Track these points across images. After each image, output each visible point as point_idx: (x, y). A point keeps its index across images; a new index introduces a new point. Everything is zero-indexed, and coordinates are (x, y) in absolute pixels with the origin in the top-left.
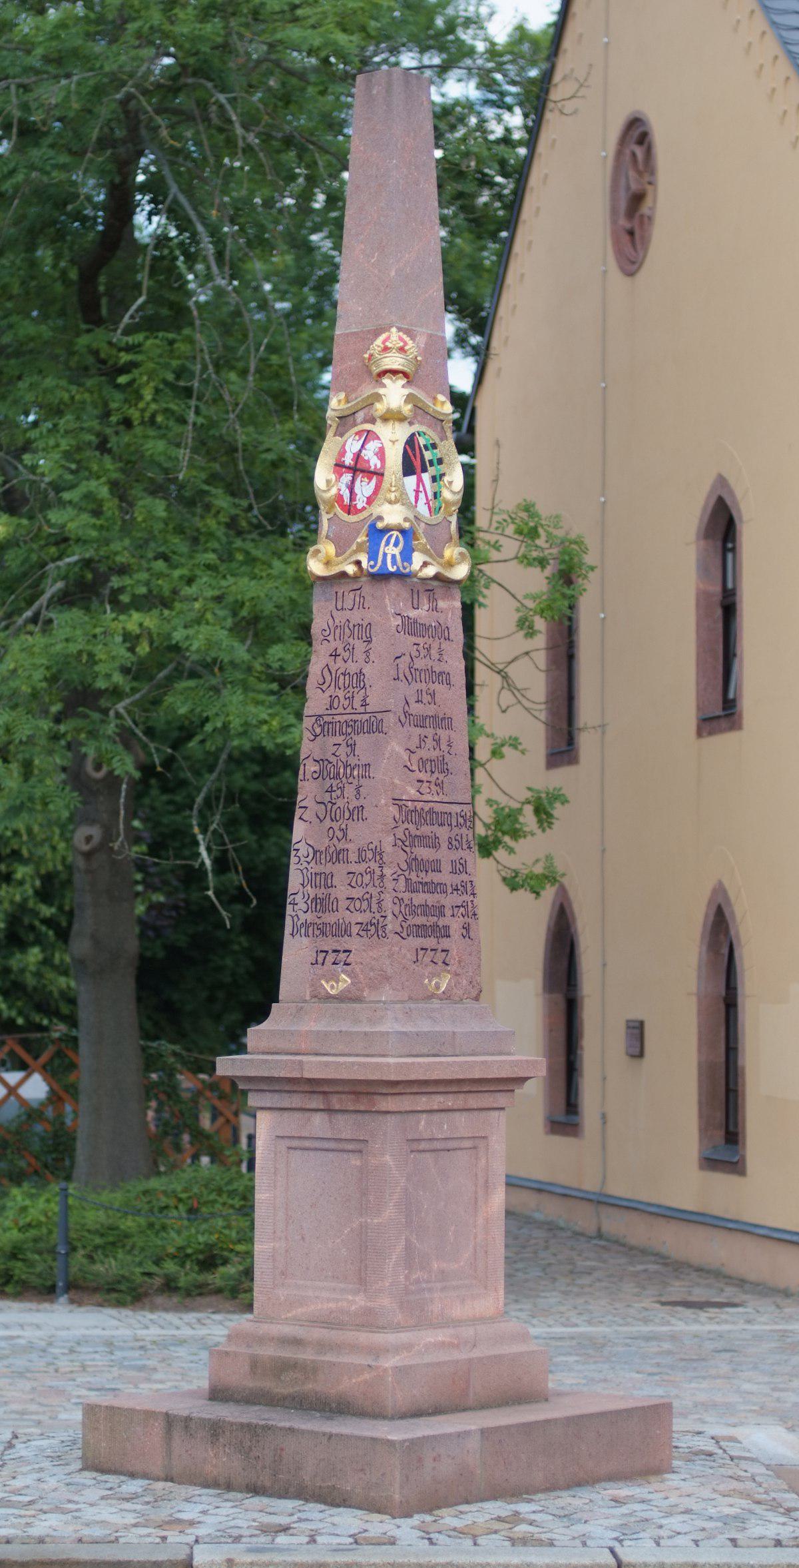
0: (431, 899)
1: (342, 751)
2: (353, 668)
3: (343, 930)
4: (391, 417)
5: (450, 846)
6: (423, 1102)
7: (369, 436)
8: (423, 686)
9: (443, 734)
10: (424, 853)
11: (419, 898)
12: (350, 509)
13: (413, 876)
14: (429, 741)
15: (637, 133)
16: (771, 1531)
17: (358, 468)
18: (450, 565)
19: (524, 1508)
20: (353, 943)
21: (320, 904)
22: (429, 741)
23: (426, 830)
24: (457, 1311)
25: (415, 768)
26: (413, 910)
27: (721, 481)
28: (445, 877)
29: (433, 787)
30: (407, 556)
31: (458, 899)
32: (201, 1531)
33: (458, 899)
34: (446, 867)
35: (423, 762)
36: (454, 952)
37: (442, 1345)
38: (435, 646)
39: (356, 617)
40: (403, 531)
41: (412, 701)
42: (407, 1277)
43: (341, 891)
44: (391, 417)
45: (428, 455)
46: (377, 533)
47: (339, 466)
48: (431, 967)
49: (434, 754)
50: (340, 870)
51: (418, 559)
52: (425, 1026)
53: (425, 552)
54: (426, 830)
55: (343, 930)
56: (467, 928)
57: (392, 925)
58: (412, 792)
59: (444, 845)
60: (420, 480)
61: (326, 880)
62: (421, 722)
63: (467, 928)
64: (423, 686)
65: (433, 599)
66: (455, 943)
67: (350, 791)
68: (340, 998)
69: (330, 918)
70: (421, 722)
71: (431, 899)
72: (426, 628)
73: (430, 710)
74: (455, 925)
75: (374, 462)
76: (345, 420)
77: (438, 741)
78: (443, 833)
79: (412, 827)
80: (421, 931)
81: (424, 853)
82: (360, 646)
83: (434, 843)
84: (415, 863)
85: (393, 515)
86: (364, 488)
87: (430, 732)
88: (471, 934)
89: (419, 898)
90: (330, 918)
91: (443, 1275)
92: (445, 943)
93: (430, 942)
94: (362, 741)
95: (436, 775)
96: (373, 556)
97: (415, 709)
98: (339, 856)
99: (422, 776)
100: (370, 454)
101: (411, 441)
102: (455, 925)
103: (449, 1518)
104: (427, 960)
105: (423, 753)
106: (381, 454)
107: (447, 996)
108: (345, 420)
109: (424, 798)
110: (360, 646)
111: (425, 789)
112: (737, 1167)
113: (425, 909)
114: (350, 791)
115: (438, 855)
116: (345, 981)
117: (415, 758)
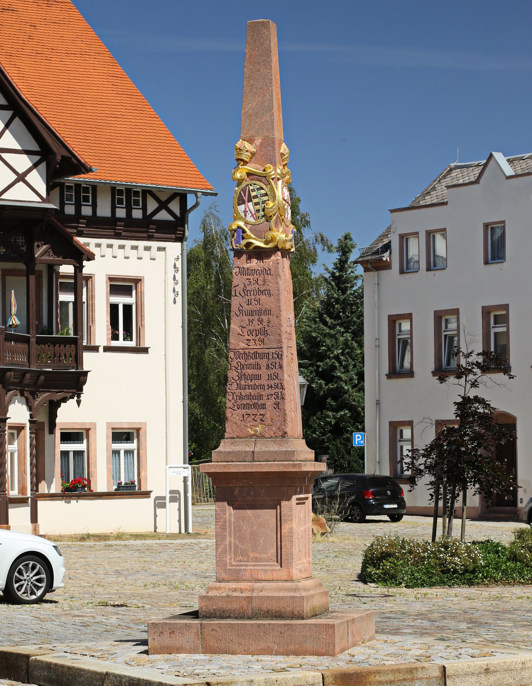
0: (253, 392)
5: (268, 367)
9: (265, 318)
10: (250, 372)
13: (243, 382)
14: (256, 322)
23: (252, 361)
24: (262, 576)
25: (246, 334)
26: (241, 397)
28: (264, 381)
29: (257, 342)
34: (265, 377)
35: (250, 332)
38: (261, 278)
41: (244, 305)
48: (254, 423)
56: (277, 404)
58: (243, 345)
66: (269, 412)
70: (251, 313)
71: (253, 392)
74: (270, 403)
77: (261, 321)
78: (263, 362)
79: (242, 361)
80: (245, 406)
83: (258, 367)
92: (262, 412)
93: (255, 411)
95: (259, 336)
97: (246, 307)
99: (249, 338)
105: (251, 328)
109: (250, 347)
111: (252, 343)
113: (249, 397)
115: (260, 372)
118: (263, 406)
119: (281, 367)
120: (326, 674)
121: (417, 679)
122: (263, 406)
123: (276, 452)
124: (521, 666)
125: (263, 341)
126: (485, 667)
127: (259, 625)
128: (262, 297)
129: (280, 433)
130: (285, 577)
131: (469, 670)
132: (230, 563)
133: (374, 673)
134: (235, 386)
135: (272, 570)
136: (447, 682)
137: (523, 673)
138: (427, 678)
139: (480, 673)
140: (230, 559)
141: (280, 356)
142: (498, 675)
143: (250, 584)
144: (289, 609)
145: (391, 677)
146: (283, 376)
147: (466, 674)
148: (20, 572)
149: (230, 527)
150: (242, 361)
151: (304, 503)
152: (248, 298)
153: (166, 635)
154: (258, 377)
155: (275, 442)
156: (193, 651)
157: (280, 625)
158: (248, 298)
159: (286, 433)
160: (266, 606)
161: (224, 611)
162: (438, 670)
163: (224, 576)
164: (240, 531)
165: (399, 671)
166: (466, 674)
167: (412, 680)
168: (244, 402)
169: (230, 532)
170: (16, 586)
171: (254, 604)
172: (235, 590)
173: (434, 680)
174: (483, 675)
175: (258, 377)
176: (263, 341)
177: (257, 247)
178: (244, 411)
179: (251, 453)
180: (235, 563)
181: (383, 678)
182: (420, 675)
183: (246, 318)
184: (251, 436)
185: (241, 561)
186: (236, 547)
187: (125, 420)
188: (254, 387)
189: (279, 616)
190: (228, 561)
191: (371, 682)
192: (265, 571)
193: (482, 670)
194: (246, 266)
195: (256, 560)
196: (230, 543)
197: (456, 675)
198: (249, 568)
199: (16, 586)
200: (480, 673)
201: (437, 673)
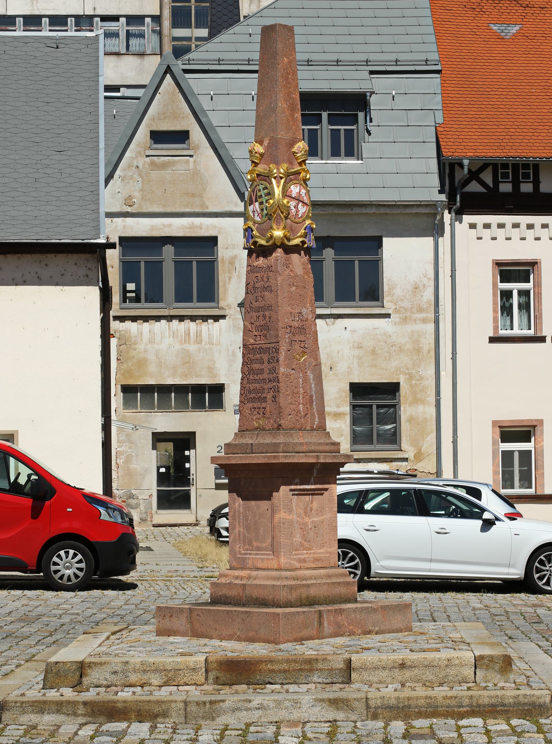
5: (269, 362)
9: (267, 313)
10: (256, 366)
13: (251, 377)
14: (261, 318)
22: (261, 318)
24: (260, 565)
25: (254, 330)
26: (250, 392)
29: (262, 337)
31: (270, 385)
33: (270, 385)
36: (268, 409)
41: (253, 302)
49: (262, 323)
58: (252, 341)
59: (266, 362)
63: (274, 397)
66: (269, 406)
70: (258, 309)
74: (269, 396)
77: (264, 316)
78: (265, 357)
81: (256, 366)
87: (261, 313)
88: (277, 400)
92: (264, 405)
95: (263, 332)
97: (256, 304)
102: (269, 396)
104: (255, 413)
105: (258, 324)
109: (257, 343)
113: (255, 390)
117: (253, 326)
118: (264, 399)
119: (278, 361)
120: (211, 659)
121: (317, 670)
122: (264, 399)
123: (268, 444)
124: (446, 662)
125: (265, 336)
126: (401, 662)
127: (228, 612)
128: (266, 293)
129: (276, 426)
130: (276, 567)
131: (379, 663)
132: (240, 551)
133: (266, 661)
135: (268, 559)
136: (352, 675)
137: (448, 670)
138: (328, 669)
139: (394, 667)
140: (240, 548)
141: (277, 351)
142: (416, 671)
143: (248, 572)
144: (271, 597)
145: (285, 666)
146: (279, 369)
147: (376, 668)
148: (542, 562)
149: (239, 517)
150: (251, 356)
151: (322, 494)
152: (256, 295)
153: (167, 618)
154: (261, 371)
155: (271, 434)
156: (183, 635)
157: (242, 612)
158: (256, 295)
159: (280, 425)
160: (256, 593)
161: (227, 598)
162: (342, 662)
163: (234, 564)
164: (247, 520)
165: (295, 661)
166: (376, 668)
167: (311, 670)
168: (252, 396)
169: (239, 522)
170: (536, 576)
171: (248, 592)
172: (237, 578)
173: (337, 672)
174: (398, 670)
175: (261, 371)
176: (265, 336)
177: (261, 246)
179: (250, 446)
180: (243, 552)
181: (276, 667)
182: (320, 666)
183: (254, 314)
184: (256, 429)
185: (247, 550)
186: (244, 536)
187: (517, 413)
189: (263, 603)
190: (238, 549)
191: (261, 670)
192: (263, 560)
193: (396, 665)
194: (256, 264)
196: (239, 531)
197: (364, 668)
198: (254, 558)
199: (536, 576)
200: (394, 667)
201: (342, 666)
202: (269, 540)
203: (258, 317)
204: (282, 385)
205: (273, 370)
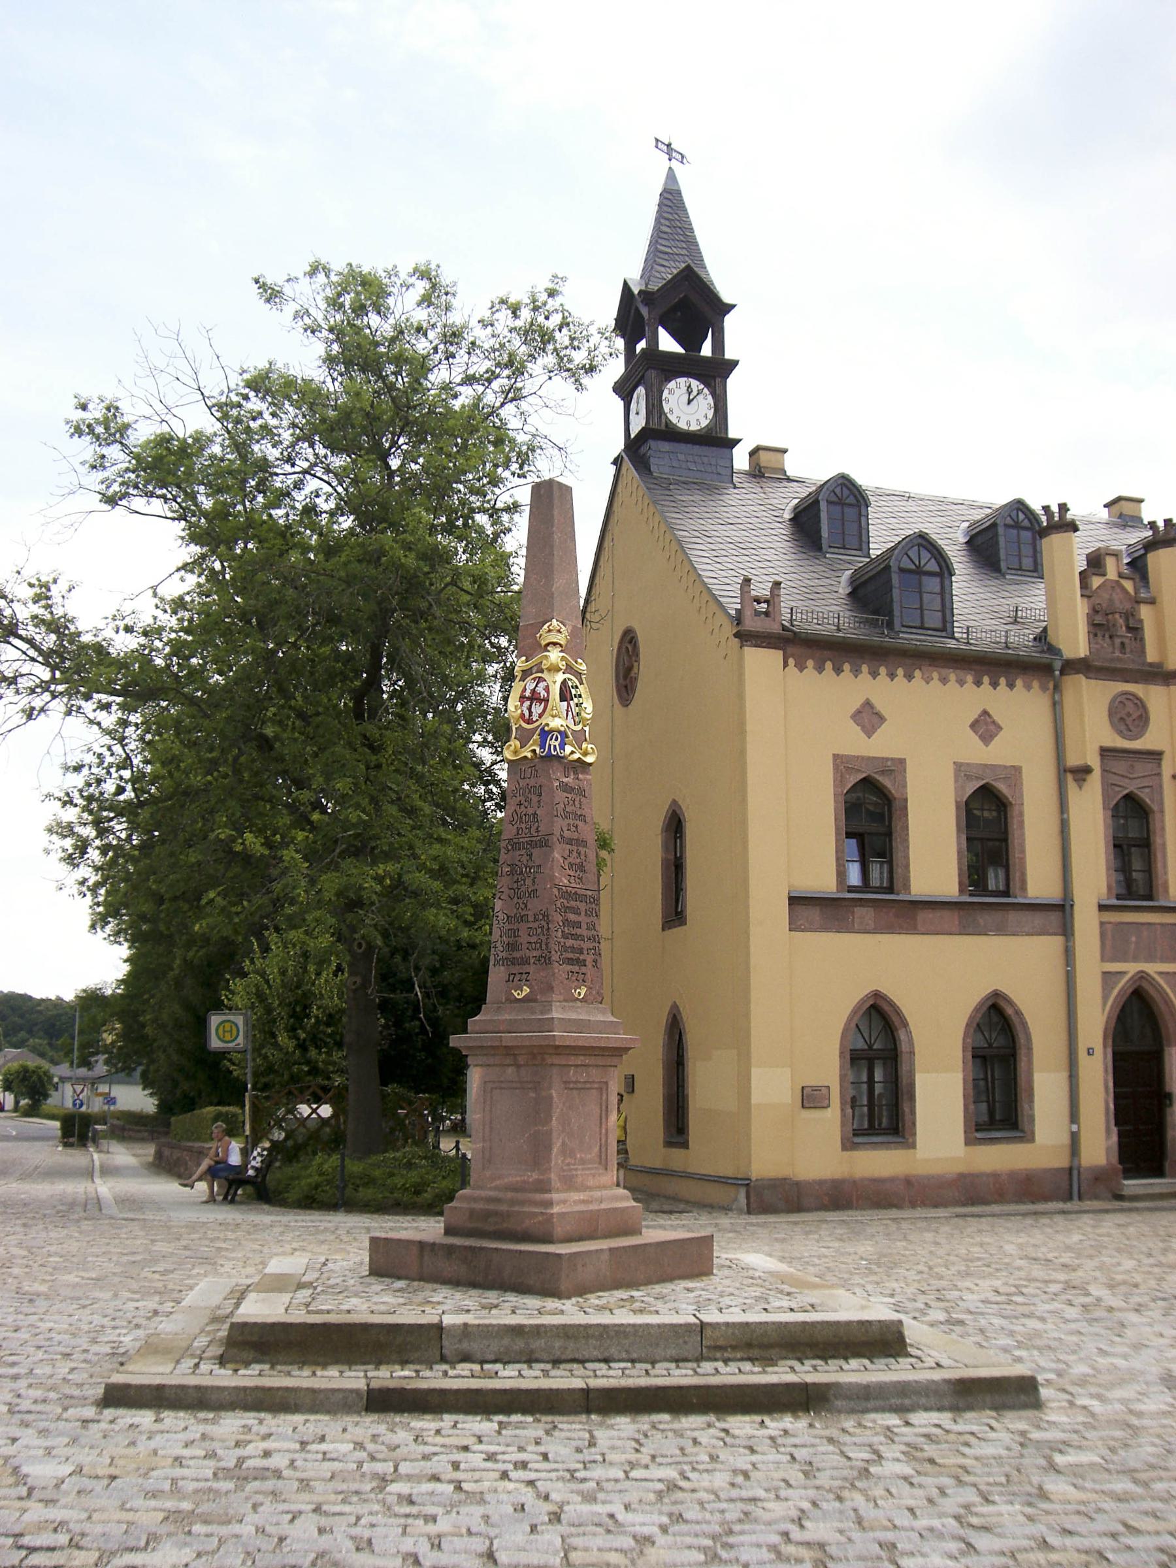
0: (576, 943)
1: (524, 859)
2: (530, 811)
3: (525, 961)
4: (555, 669)
6: (573, 1060)
7: (541, 679)
8: (571, 822)
10: (572, 917)
11: (570, 943)
12: (529, 722)
14: (575, 853)
15: (629, 639)
16: (785, 1303)
17: (534, 698)
18: (586, 754)
19: (635, 1293)
20: (531, 969)
21: (511, 947)
22: (575, 853)
23: (573, 903)
24: (591, 1183)
26: (566, 949)
27: (674, 802)
30: (562, 747)
32: (445, 1308)
34: (584, 926)
37: (583, 1202)
39: (532, 782)
40: (560, 732)
41: (565, 829)
42: (563, 1161)
43: (524, 938)
44: (555, 669)
45: (573, 691)
46: (545, 734)
47: (522, 698)
48: (576, 983)
50: (523, 927)
51: (568, 749)
52: (574, 1016)
53: (573, 745)
54: (573, 903)
55: (525, 961)
56: (595, 961)
57: (555, 957)
59: (583, 913)
60: (569, 705)
61: (515, 933)
62: (570, 842)
63: (595, 961)
64: (571, 822)
65: (576, 773)
66: (589, 970)
67: (529, 881)
68: (526, 999)
69: (516, 955)
70: (570, 842)
71: (576, 943)
72: (573, 789)
73: (575, 836)
75: (543, 694)
76: (526, 673)
80: (570, 961)
81: (572, 917)
82: (535, 799)
83: (577, 911)
84: (566, 922)
85: (556, 723)
86: (537, 709)
87: (575, 848)
89: (570, 943)
90: (516, 955)
91: (583, 1162)
92: (584, 969)
93: (576, 968)
94: (536, 852)
96: (542, 746)
97: (566, 834)
98: (522, 918)
99: (570, 873)
100: (540, 689)
101: (564, 682)
102: (589, 959)
103: (593, 1299)
105: (570, 860)
106: (547, 689)
107: (584, 1000)
108: (526, 673)
110: (535, 799)
112: (685, 1145)
113: (573, 949)
114: (529, 881)
115: (580, 919)
116: (526, 990)
122: (583, 963)
128: (580, 824)
134: (560, 933)
168: (571, 955)
175: (578, 925)
178: (569, 968)
188: (575, 937)
195: (583, 1162)
202: (597, 1149)
203: (571, 852)
204: (604, 946)
205: (592, 926)
